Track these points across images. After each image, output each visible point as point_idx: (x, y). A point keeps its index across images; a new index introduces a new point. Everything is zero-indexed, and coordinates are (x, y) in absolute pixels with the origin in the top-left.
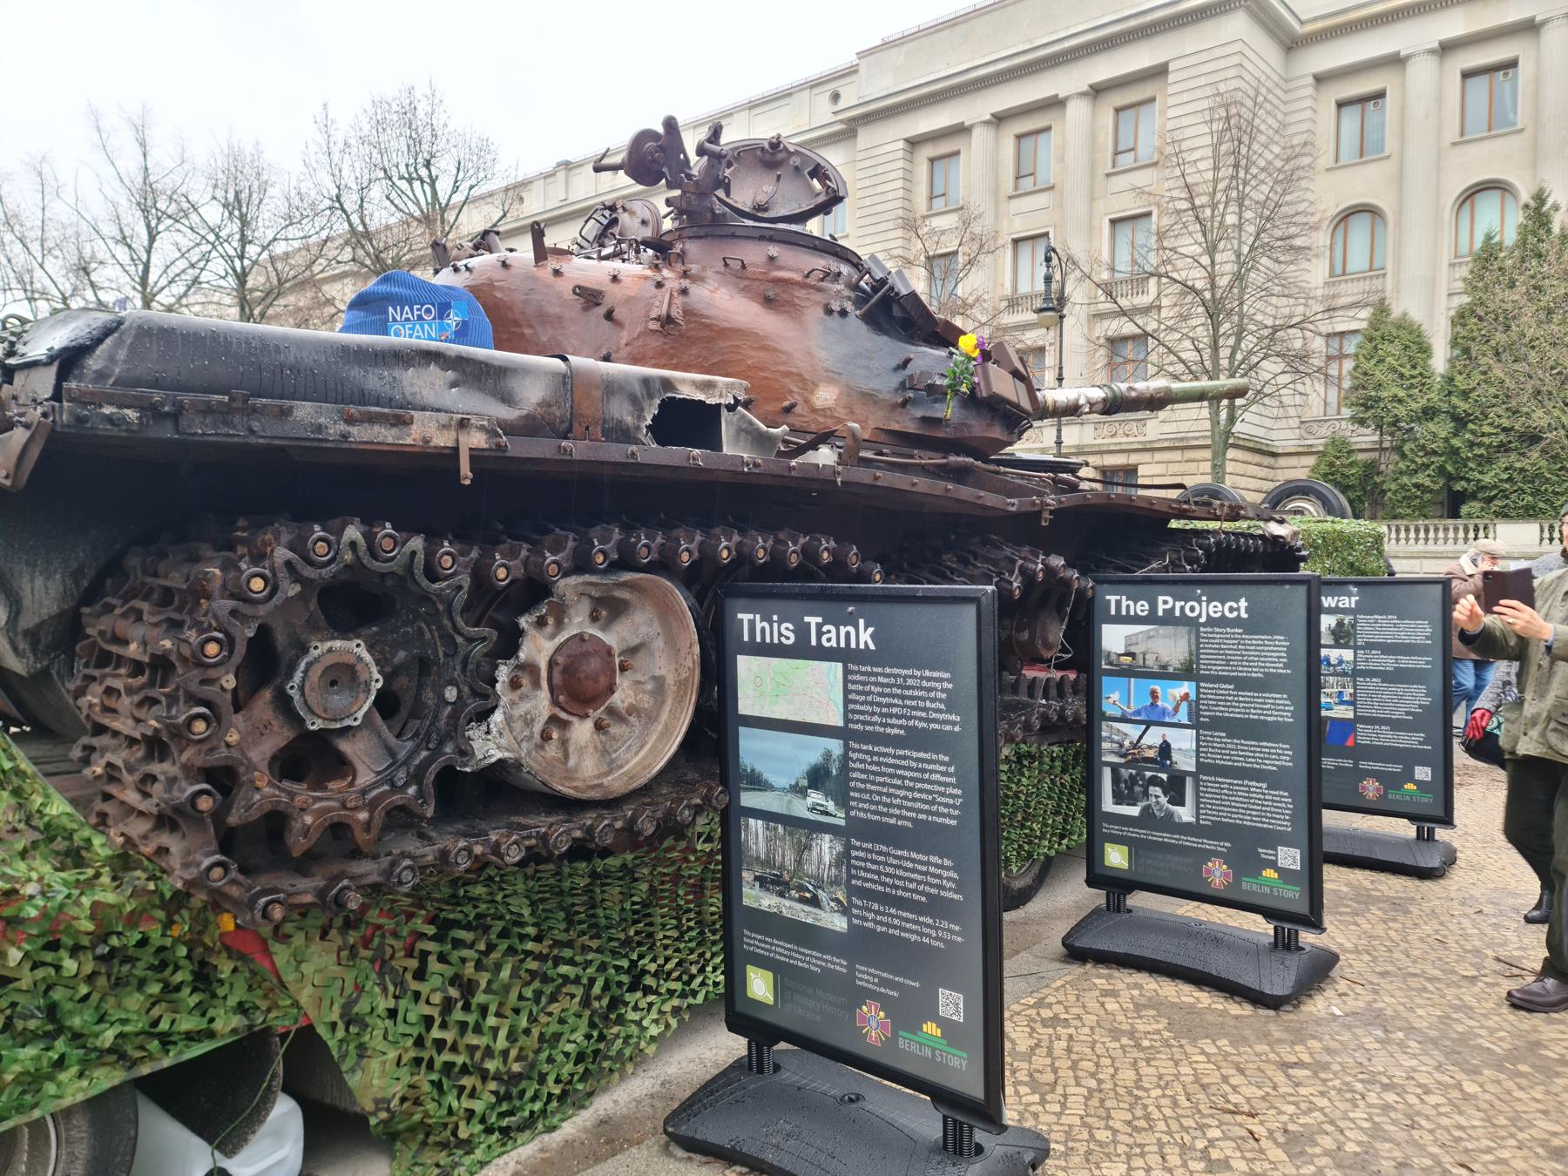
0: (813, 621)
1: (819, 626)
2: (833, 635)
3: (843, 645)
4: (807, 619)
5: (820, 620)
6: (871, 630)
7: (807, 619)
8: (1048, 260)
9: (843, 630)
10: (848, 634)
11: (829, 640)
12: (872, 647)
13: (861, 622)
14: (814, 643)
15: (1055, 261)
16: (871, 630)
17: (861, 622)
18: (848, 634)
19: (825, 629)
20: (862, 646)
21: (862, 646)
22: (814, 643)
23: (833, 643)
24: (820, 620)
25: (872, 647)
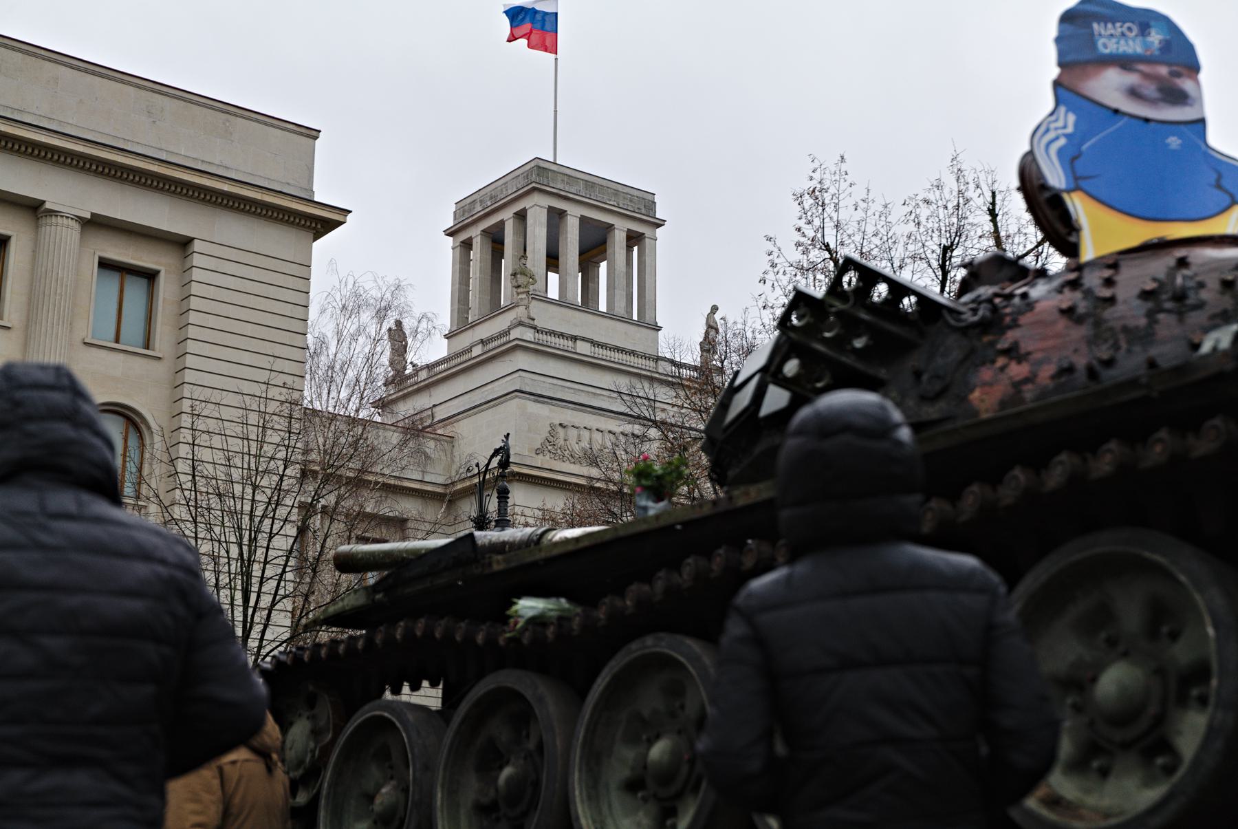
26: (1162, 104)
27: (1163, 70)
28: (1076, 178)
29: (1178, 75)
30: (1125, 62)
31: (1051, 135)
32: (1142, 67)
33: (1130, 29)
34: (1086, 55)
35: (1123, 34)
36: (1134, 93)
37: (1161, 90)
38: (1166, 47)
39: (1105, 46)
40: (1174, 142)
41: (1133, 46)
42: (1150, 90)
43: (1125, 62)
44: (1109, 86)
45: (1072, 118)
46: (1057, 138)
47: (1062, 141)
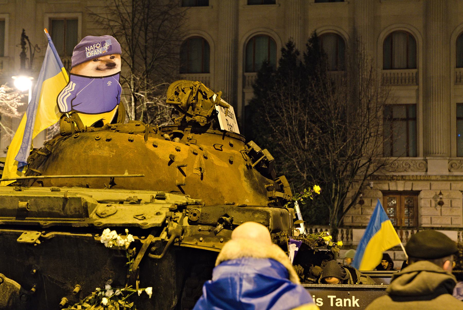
0: (332, 297)
1: (334, 299)
2: (341, 302)
3: (345, 305)
4: (329, 297)
5: (335, 297)
6: (357, 300)
7: (329, 297)
8: (23, 44)
9: (345, 300)
10: (347, 302)
11: (339, 304)
12: (358, 306)
13: (353, 297)
14: (332, 305)
15: (27, 45)
16: (357, 300)
17: (353, 297)
18: (347, 302)
19: (337, 300)
20: (354, 306)
21: (354, 306)
22: (332, 305)
23: (341, 305)
24: (335, 297)
25: (358, 306)
26: (107, 70)
27: (108, 57)
28: (72, 106)
29: (113, 58)
30: (95, 59)
31: (66, 93)
32: (101, 58)
33: (98, 45)
34: (84, 60)
35: (96, 48)
36: (98, 69)
37: (107, 65)
38: (110, 48)
39: (89, 55)
40: (109, 83)
41: (99, 51)
42: (103, 66)
43: (95, 59)
44: (89, 69)
45: (74, 84)
46: (68, 93)
47: (70, 94)
